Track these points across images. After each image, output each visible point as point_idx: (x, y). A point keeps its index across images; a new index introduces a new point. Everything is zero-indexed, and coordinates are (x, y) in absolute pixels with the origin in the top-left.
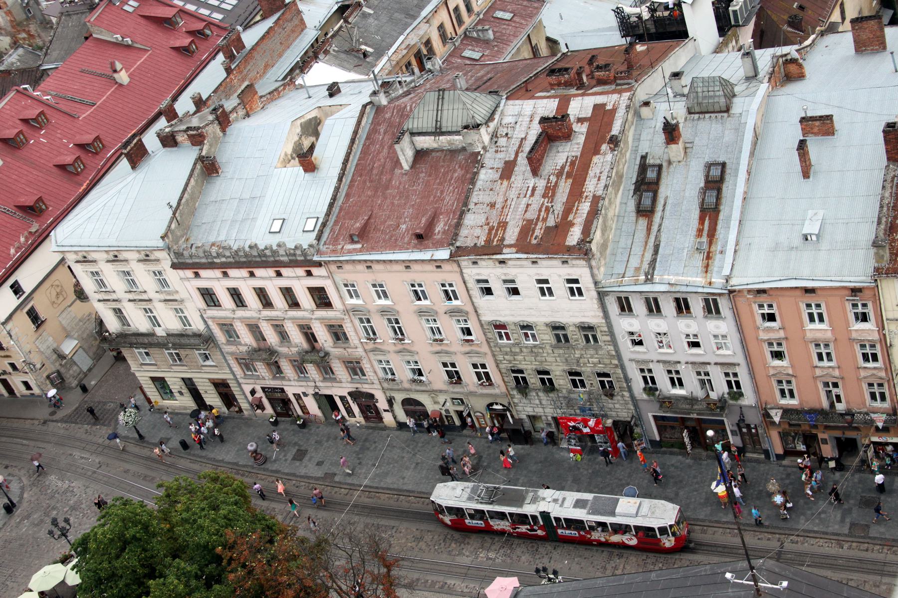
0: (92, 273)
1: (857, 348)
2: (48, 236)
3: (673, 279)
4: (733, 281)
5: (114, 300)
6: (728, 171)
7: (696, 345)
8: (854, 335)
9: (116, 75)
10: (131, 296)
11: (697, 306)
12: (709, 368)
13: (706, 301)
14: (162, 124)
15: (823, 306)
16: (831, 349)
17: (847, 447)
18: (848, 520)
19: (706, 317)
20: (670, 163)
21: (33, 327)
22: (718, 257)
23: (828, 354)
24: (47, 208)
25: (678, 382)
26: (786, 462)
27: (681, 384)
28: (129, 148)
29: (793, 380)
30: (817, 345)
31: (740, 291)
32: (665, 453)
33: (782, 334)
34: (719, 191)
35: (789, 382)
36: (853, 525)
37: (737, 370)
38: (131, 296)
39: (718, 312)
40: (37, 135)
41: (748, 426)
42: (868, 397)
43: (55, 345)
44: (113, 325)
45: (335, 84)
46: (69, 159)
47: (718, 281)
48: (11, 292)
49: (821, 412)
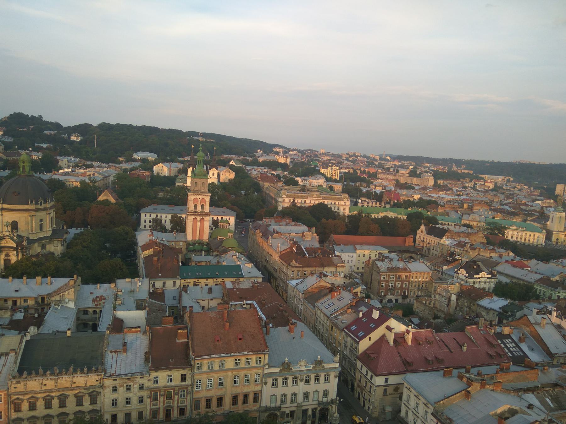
0: (408, 394)
2: (405, 374)
5: (408, 408)
9: (463, 347)
10: (414, 411)
14: (463, 371)
21: (383, 394)
24: (413, 366)
28: (447, 369)
38: (414, 411)
40: (426, 345)
43: (384, 405)
44: (403, 414)
45: (532, 405)
46: (429, 358)
48: (384, 380)
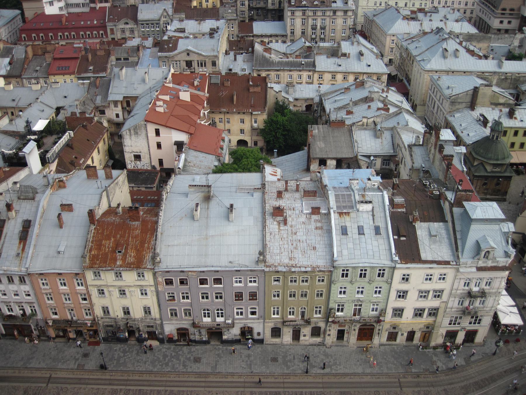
1: (79, 296)
3: (5, 268)
4: (29, 270)
6: (32, 224)
7: (17, 295)
8: (78, 291)
11: (16, 280)
12: (23, 304)
13: (20, 277)
15: (65, 280)
16: (70, 296)
17: (79, 333)
18: (77, 363)
19: (20, 284)
20: (9, 219)
22: (25, 260)
23: (69, 298)
25: (10, 310)
26: (56, 340)
27: (12, 310)
29: (57, 309)
30: (65, 295)
31: (33, 274)
32: (7, 339)
33: (51, 291)
34: (28, 232)
35: (55, 309)
36: (79, 365)
37: (34, 305)
39: (25, 282)
41: (41, 327)
42: (85, 314)
47: (23, 269)
49: (68, 321)
